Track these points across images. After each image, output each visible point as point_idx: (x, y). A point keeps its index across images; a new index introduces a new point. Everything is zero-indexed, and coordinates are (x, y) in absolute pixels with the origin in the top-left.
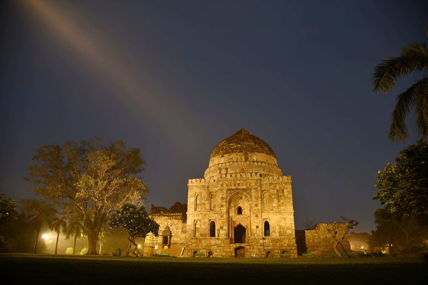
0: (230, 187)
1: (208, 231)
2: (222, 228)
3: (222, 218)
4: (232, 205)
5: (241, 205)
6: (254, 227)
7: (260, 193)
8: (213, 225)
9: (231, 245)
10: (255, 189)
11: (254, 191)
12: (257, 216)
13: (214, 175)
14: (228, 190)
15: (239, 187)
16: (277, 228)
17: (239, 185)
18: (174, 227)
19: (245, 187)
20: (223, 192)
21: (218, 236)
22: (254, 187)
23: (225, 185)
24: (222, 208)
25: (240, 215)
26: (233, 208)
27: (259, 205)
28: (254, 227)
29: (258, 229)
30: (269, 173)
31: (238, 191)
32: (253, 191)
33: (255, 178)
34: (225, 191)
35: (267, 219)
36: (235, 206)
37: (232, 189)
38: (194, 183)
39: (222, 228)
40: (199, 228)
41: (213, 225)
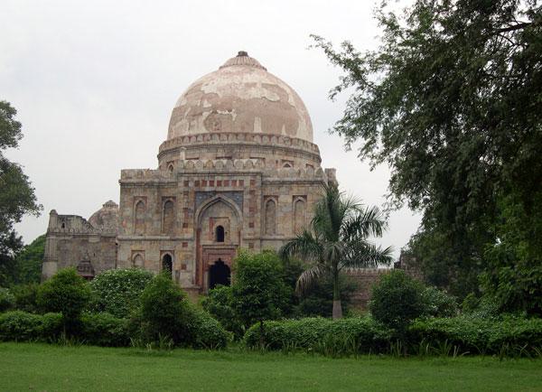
2: (184, 267)
3: (185, 249)
4: (206, 222)
7: (259, 201)
8: (167, 261)
10: (252, 192)
11: (248, 197)
13: (174, 158)
15: (219, 189)
17: (219, 183)
18: (101, 259)
19: (230, 188)
22: (248, 189)
23: (191, 184)
26: (208, 230)
27: (258, 225)
30: (285, 158)
31: (217, 196)
32: (247, 197)
36: (211, 228)
37: (205, 193)
38: (131, 178)
39: (184, 267)
41: (167, 261)
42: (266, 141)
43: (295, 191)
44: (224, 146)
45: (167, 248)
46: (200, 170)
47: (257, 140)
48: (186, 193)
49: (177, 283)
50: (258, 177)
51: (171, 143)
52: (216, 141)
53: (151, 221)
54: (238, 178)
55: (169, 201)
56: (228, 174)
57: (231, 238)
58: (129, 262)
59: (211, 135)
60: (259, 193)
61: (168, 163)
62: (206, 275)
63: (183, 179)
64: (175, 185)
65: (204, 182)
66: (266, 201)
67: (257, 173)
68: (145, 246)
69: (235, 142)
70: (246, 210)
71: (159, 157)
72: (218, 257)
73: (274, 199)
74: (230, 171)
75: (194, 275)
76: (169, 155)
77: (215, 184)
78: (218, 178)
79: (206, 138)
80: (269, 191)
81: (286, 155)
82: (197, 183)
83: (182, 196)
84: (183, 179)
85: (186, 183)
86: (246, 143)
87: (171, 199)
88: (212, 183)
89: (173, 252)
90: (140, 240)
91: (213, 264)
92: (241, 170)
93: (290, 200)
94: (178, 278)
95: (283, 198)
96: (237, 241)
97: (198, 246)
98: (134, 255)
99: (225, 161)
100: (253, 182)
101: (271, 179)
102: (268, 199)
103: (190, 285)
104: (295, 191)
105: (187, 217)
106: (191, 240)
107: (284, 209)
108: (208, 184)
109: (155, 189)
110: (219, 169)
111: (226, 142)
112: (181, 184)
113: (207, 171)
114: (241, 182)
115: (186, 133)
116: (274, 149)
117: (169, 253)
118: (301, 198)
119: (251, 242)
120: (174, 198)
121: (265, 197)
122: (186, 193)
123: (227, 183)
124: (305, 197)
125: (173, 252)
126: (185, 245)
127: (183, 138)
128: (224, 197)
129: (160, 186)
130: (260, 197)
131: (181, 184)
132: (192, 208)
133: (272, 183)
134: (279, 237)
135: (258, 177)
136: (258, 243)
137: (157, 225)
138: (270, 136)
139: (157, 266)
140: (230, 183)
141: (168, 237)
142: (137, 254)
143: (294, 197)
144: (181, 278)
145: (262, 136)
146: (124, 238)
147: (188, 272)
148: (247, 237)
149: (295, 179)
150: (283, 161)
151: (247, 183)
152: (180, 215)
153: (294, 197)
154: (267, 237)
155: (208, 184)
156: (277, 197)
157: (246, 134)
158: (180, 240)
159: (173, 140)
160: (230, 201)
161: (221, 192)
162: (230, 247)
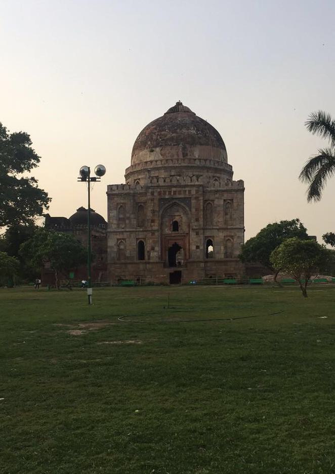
0: (163, 196)
1: (135, 254)
3: (153, 237)
5: (177, 219)
6: (193, 248)
7: (202, 204)
8: (141, 246)
9: (166, 269)
10: (197, 198)
12: (197, 234)
13: (140, 177)
14: (160, 200)
15: (175, 197)
16: (222, 248)
17: (175, 193)
20: (154, 203)
21: (149, 259)
23: (156, 194)
24: (153, 224)
25: (177, 232)
26: (167, 224)
27: (201, 220)
28: (193, 248)
29: (198, 250)
30: (215, 175)
31: (173, 202)
32: (193, 201)
33: (197, 183)
34: (156, 201)
35: (210, 237)
38: (114, 190)
39: (153, 249)
40: (123, 250)
41: (141, 246)
42: (203, 163)
43: (226, 196)
44: (175, 168)
45: (140, 237)
46: (161, 183)
47: (197, 163)
48: (152, 200)
49: (149, 259)
50: (201, 188)
51: (137, 165)
52: (171, 165)
53: (129, 218)
54: (187, 189)
55: (141, 205)
56: (181, 186)
57: (184, 228)
58: (115, 247)
59: (167, 160)
60: (201, 198)
61: (135, 180)
62: (167, 252)
63: (150, 190)
64: (146, 193)
65: (165, 193)
66: (206, 204)
67: (201, 185)
68: (125, 235)
69: (183, 164)
70: (193, 210)
71: (127, 176)
72: (174, 242)
73: (211, 203)
74: (182, 184)
75: (160, 254)
76: (136, 175)
77: (172, 194)
78: (174, 189)
79: (163, 163)
80: (212, 198)
81: (216, 173)
82: (160, 193)
83: (150, 202)
84: (150, 190)
85: (152, 194)
86: (190, 165)
87: (142, 204)
88: (170, 192)
89: (145, 239)
90: (123, 232)
91: (171, 246)
92: (189, 184)
93: (222, 202)
94: (149, 256)
95: (216, 202)
96: (187, 229)
97: (161, 235)
98: (119, 242)
99: (178, 177)
100: (197, 192)
101: (209, 189)
102: (208, 202)
103: (157, 260)
104: (226, 196)
105: (154, 215)
106: (157, 231)
107: (218, 209)
108: (167, 193)
109: (132, 198)
110: (175, 183)
111: (177, 165)
112: (149, 194)
113: (167, 184)
114: (190, 191)
115: (148, 159)
116: (208, 169)
117: (142, 240)
118: (230, 201)
119: (197, 231)
120: (145, 203)
121: (206, 201)
122: (152, 200)
123: (180, 193)
124: (232, 200)
125: (145, 239)
126: (153, 234)
127: (146, 162)
128: (177, 201)
129: (134, 195)
130: (202, 201)
131: (149, 194)
132: (157, 210)
133: (211, 191)
134: (215, 227)
135: (201, 188)
136: (202, 231)
137: (134, 222)
138: (206, 160)
139: (134, 248)
140: (182, 192)
141: (141, 230)
142: (120, 241)
143: (224, 200)
144: (151, 255)
145: (200, 160)
146: (112, 230)
147: (156, 252)
148: (194, 227)
149: (225, 189)
150: (214, 177)
151: (193, 192)
152: (149, 215)
153: (224, 200)
154: (207, 227)
155: (167, 193)
156: (213, 201)
157: (190, 159)
158: (150, 231)
159: (139, 164)
160: (182, 204)
161: (176, 198)
162: (183, 235)
